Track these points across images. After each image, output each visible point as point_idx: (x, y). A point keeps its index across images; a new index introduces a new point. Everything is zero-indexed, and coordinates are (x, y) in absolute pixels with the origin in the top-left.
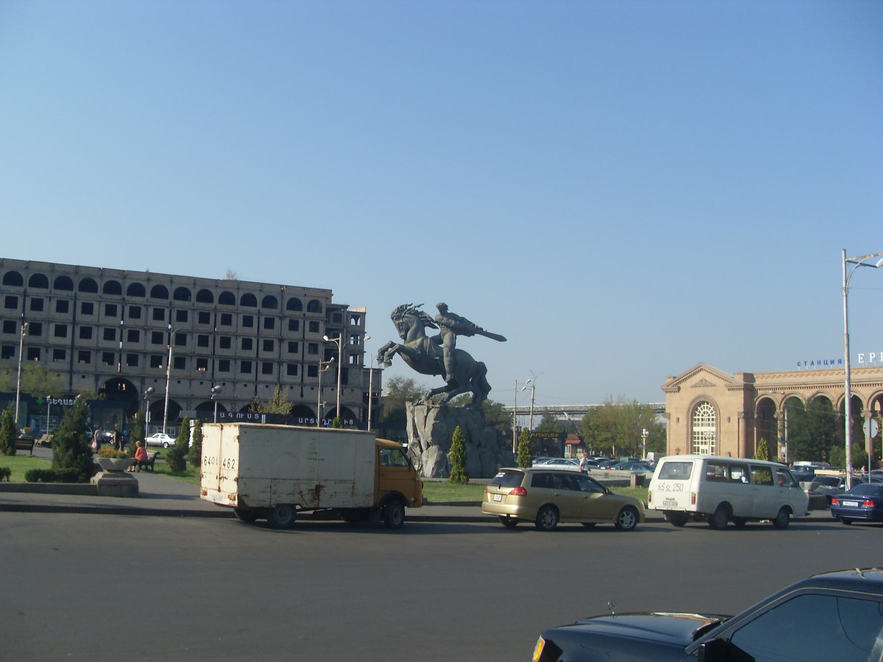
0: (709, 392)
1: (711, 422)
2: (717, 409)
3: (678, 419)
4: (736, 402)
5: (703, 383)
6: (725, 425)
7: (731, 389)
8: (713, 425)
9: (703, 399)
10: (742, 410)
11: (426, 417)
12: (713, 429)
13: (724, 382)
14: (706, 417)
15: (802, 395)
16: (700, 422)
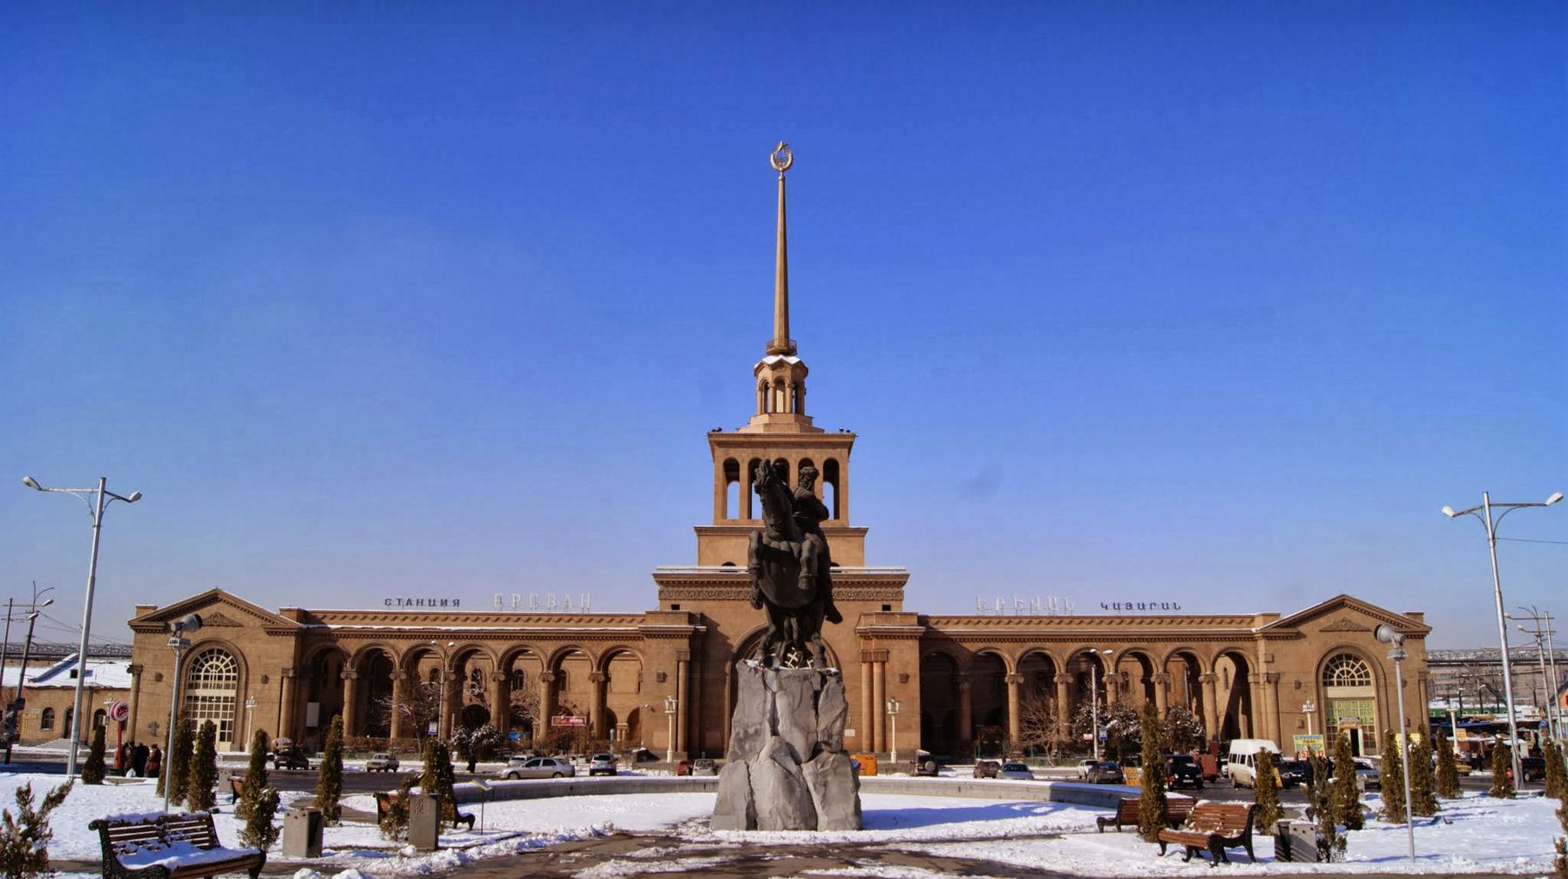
0: (227, 634)
1: (223, 682)
2: (240, 666)
3: (159, 677)
4: (283, 652)
5: (219, 621)
6: (255, 685)
7: (272, 632)
8: (227, 687)
9: (215, 647)
10: (290, 665)
11: (816, 695)
12: (231, 693)
13: (259, 622)
14: (214, 672)
15: (393, 647)
16: (202, 681)
